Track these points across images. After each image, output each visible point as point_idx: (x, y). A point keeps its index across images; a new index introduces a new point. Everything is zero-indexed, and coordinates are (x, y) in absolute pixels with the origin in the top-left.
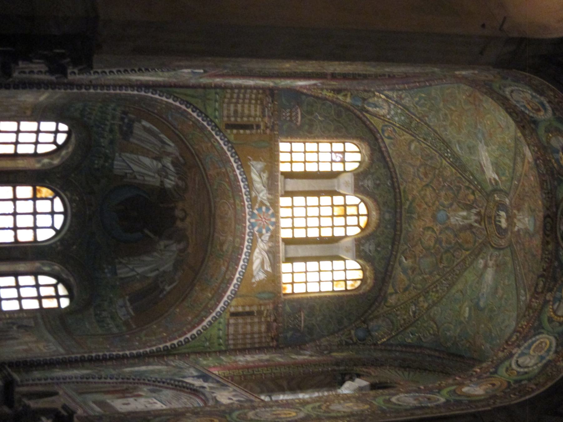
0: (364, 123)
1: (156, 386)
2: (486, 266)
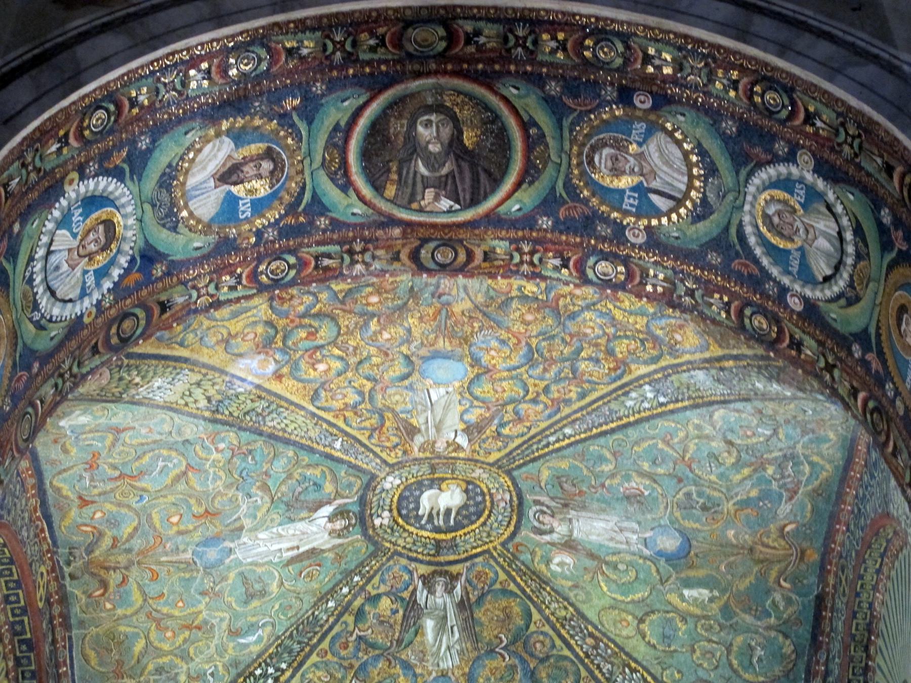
2: (569, 545)
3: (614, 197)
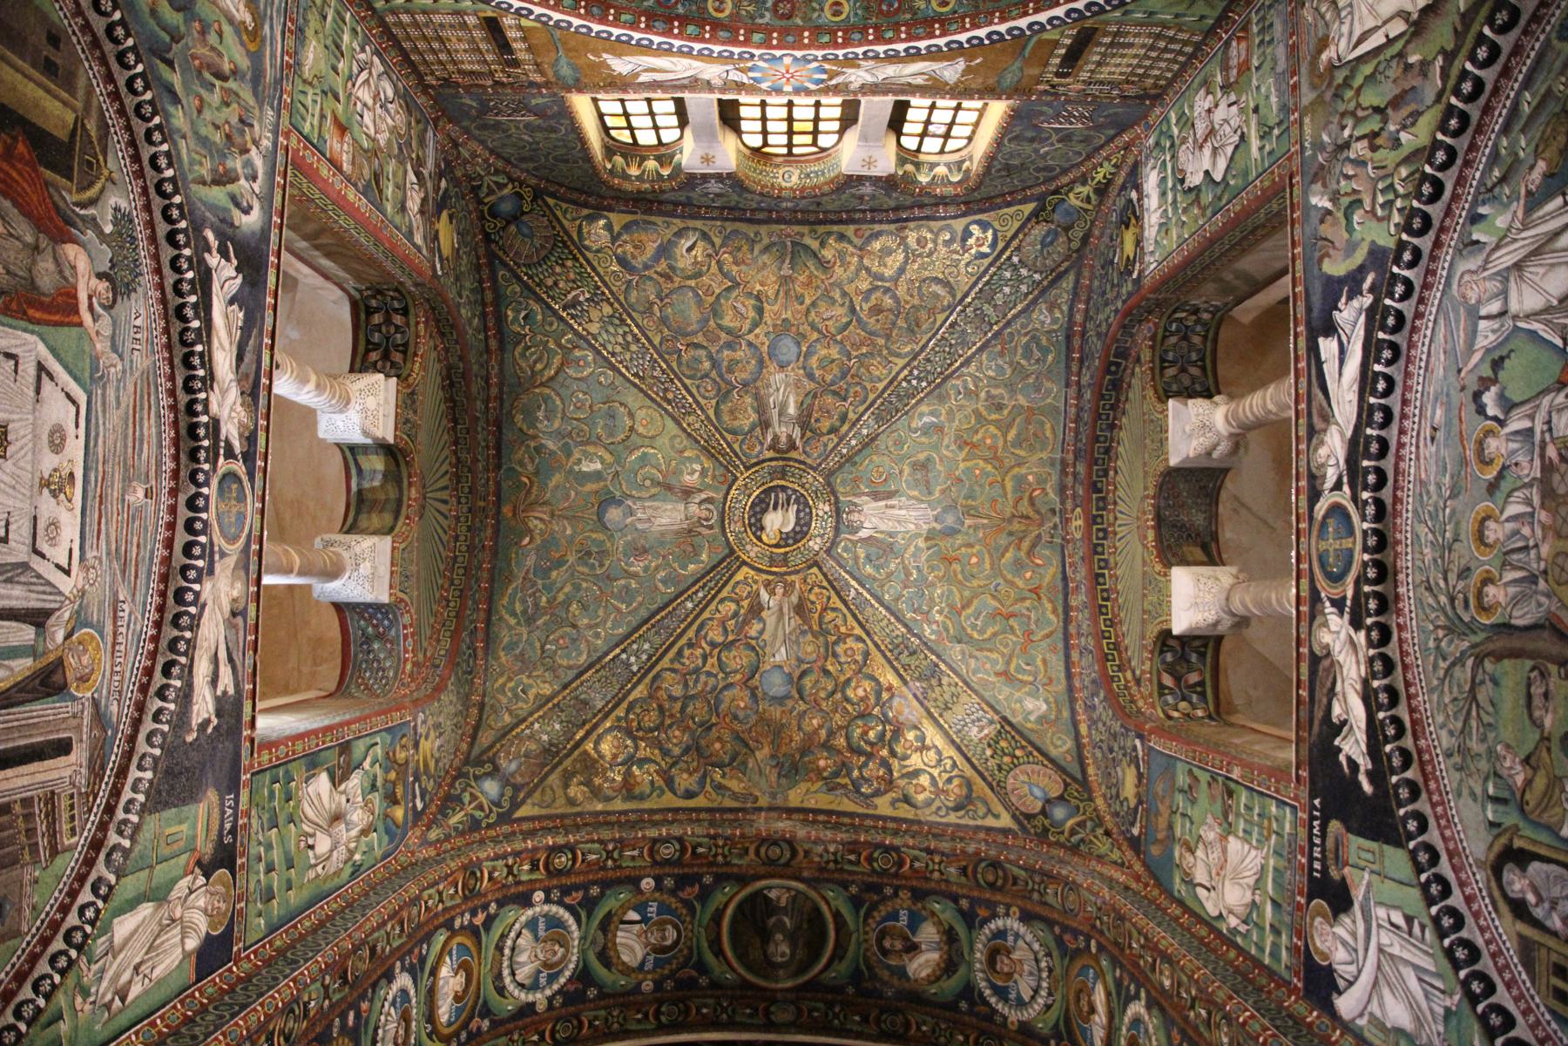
0: (1010, 193)
1: (148, 208)
2: (687, 493)
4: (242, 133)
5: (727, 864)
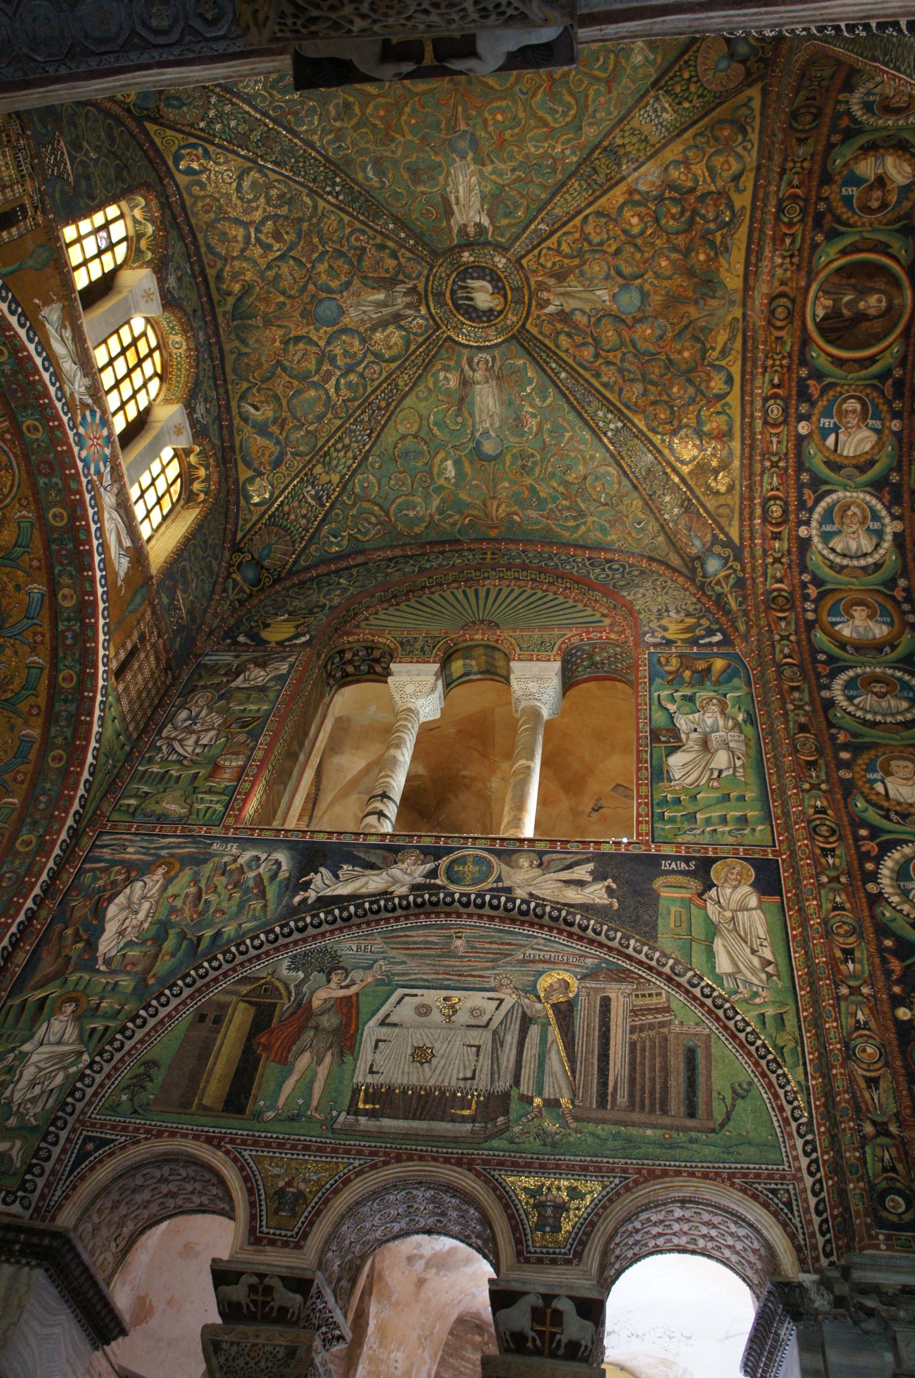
0: (141, 146)
1: (286, 946)
2: (465, 383)
3: (827, 414)
4: (231, 871)
5: (790, 356)
